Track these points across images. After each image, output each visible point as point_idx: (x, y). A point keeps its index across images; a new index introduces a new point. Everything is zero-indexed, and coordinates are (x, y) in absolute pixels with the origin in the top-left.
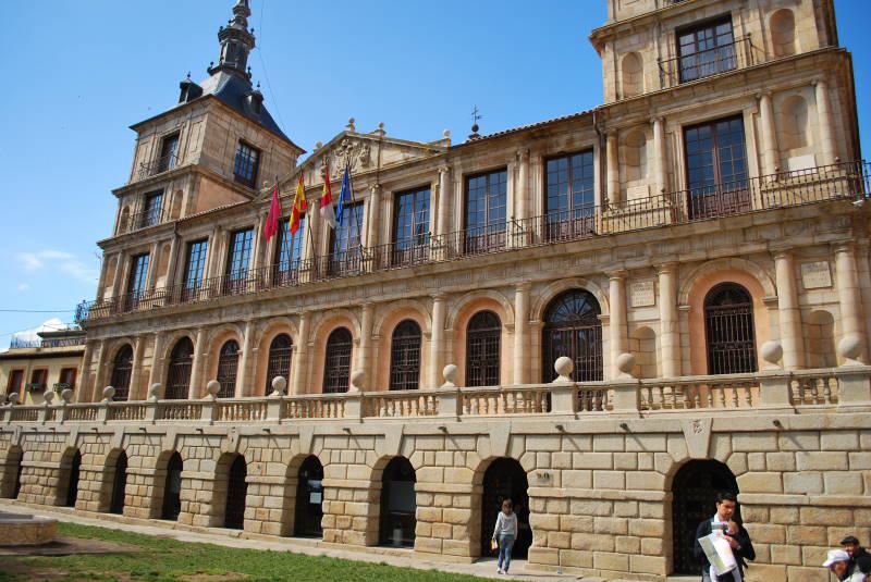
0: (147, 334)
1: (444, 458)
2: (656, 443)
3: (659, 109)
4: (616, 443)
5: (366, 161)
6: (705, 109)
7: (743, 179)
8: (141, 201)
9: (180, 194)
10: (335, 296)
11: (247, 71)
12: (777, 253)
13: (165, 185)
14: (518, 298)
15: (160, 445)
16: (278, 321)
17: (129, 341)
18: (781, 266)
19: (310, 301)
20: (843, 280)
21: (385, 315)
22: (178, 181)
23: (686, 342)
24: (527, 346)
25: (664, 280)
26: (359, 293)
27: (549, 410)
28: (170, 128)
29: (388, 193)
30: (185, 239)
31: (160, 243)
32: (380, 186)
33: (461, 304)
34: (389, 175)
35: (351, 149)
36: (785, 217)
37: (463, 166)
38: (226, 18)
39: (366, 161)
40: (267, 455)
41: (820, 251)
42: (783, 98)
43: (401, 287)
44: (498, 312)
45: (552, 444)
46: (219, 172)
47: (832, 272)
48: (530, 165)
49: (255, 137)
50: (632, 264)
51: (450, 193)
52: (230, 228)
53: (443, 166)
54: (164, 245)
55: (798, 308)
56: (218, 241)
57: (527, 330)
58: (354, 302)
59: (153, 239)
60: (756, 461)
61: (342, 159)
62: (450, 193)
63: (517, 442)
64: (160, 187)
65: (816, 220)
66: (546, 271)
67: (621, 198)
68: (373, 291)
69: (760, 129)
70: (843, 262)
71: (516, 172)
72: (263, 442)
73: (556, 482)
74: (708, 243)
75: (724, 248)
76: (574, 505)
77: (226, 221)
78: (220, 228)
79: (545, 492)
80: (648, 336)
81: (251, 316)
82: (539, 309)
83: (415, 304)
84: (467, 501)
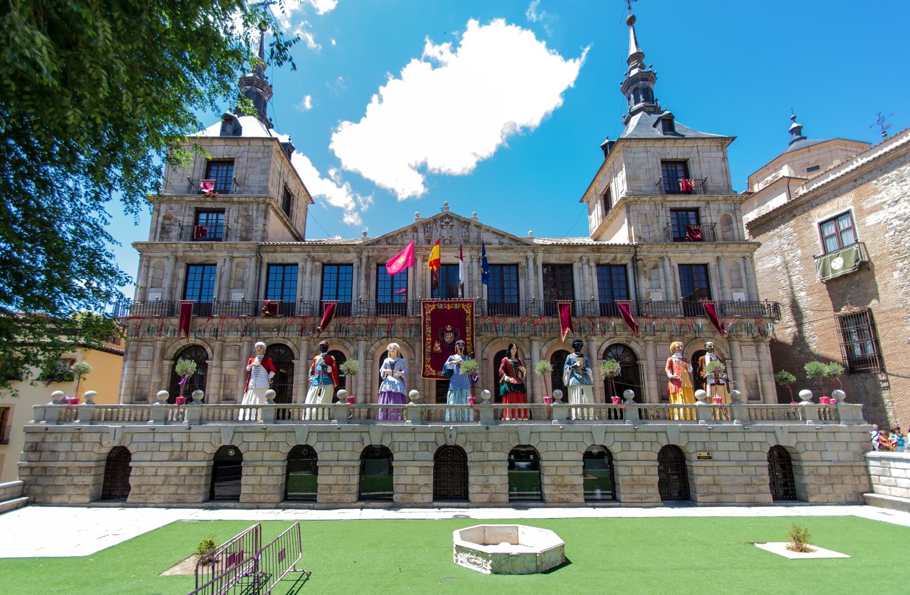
8: (192, 213)
9: (248, 218)
15: (362, 440)
22: (245, 206)
31: (232, 258)
35: (452, 226)
48: (590, 267)
51: (536, 273)
52: (325, 261)
53: (530, 254)
54: (236, 261)
56: (312, 269)
62: (536, 273)
64: (219, 206)
78: (314, 260)
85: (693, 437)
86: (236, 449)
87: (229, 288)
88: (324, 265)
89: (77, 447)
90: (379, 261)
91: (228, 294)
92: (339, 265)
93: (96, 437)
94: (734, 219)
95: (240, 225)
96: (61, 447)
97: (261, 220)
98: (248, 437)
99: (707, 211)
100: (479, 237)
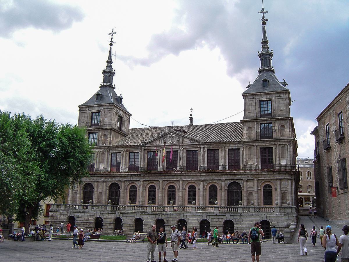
0: (99, 181)
1: (216, 220)
2: (258, 218)
3: (256, 143)
4: (251, 218)
5: (178, 141)
6: (265, 145)
7: (272, 162)
9: (105, 135)
10: (171, 177)
11: (113, 86)
12: (277, 179)
13: (98, 131)
14: (223, 183)
16: (151, 182)
17: (91, 182)
18: (279, 182)
19: (163, 178)
20: (289, 187)
21: (186, 184)
23: (259, 196)
24: (225, 194)
25: (256, 182)
26: (179, 177)
27: (238, 211)
28: (96, 109)
29: (185, 151)
30: (111, 152)
32: (183, 148)
33: (207, 183)
34: (186, 146)
36: (280, 172)
37: (207, 147)
38: (104, 66)
39: (178, 141)
40: (171, 219)
41: (285, 180)
42: (282, 146)
43: (191, 177)
44: (216, 185)
45: (239, 218)
46: (114, 127)
47: (288, 185)
49: (122, 114)
50: (248, 178)
53: (202, 147)
55: (281, 191)
57: (225, 191)
58: (177, 179)
59: (98, 150)
60: (274, 221)
61: (170, 139)
63: (232, 217)
65: (285, 174)
66: (231, 177)
67: (247, 163)
68: (183, 177)
69: (277, 152)
70: (290, 183)
71: (221, 151)
72: (169, 216)
73: (239, 224)
74: (265, 176)
75: (268, 177)
76: (243, 228)
77: (128, 149)
79: (238, 226)
80: (251, 193)
81: (142, 180)
82: (227, 185)
83: (195, 182)
84: (222, 228)
85: (234, 217)
86: (101, 218)
87: (99, 162)
88: (130, 153)
89: (62, 216)
90: (148, 151)
91: (99, 165)
92: (135, 152)
93: (66, 213)
94: (286, 127)
95: (102, 138)
96: (59, 215)
97: (109, 136)
98: (104, 215)
99: (275, 124)
100: (183, 140)
